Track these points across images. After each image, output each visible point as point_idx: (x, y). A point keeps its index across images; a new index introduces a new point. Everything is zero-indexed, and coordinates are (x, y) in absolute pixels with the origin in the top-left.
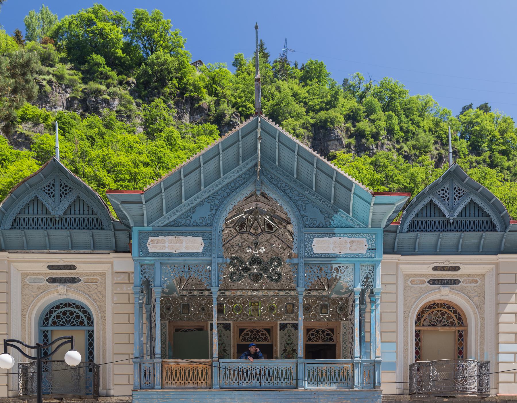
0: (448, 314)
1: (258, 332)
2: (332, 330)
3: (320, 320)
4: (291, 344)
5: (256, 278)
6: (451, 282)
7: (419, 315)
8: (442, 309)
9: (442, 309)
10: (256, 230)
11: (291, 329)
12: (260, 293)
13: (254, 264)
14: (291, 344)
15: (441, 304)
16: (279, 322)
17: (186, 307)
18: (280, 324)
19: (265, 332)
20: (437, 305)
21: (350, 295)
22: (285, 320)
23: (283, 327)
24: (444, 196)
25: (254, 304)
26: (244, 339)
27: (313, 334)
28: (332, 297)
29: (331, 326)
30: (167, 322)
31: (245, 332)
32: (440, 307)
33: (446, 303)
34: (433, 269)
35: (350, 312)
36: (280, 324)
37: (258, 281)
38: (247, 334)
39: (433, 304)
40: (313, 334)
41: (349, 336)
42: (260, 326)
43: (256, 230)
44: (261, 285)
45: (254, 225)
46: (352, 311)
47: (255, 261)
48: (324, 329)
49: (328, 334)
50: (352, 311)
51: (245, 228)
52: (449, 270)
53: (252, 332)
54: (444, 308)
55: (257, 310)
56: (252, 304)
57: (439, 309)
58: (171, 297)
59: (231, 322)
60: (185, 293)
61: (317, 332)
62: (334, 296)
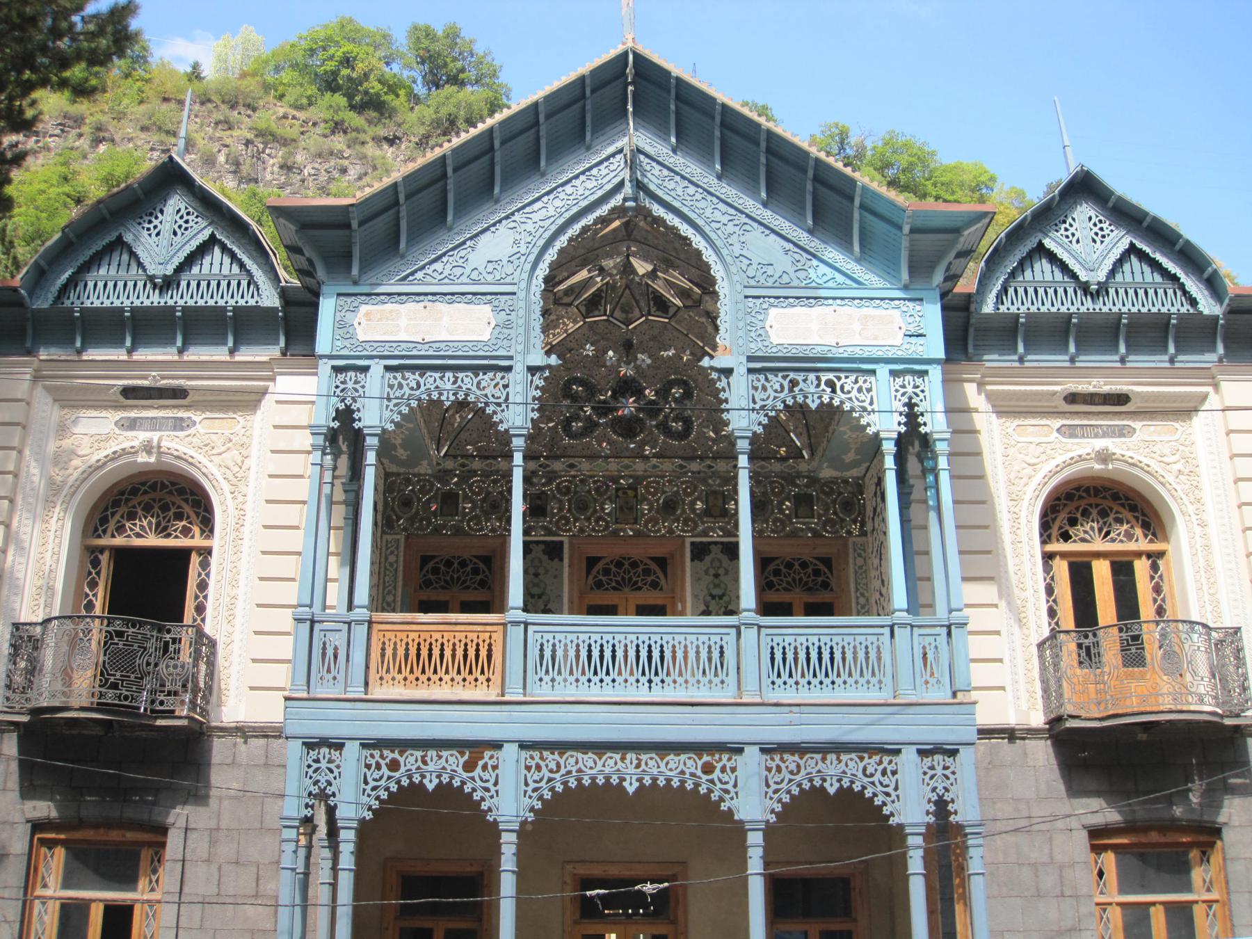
0: (1117, 512)
1: (634, 565)
2: (827, 562)
3: (794, 534)
4: (721, 597)
5: (628, 428)
6: (1113, 432)
7: (1044, 515)
8: (1099, 501)
9: (1099, 501)
10: (627, 312)
11: (720, 556)
12: (639, 467)
13: (623, 395)
14: (721, 597)
15: (1095, 488)
16: (688, 541)
17: (450, 501)
18: (692, 544)
19: (653, 566)
20: (1087, 490)
21: (868, 469)
22: (705, 533)
23: (700, 552)
24: (1069, 233)
25: (625, 493)
26: (599, 585)
27: (777, 573)
28: (821, 475)
29: (823, 551)
30: (402, 537)
31: (600, 565)
32: (1096, 496)
33: (1107, 484)
34: (1065, 399)
35: (869, 512)
36: (692, 544)
37: (636, 435)
38: (606, 572)
39: (1078, 489)
40: (777, 573)
41: (873, 573)
42: (638, 551)
43: (627, 312)
44: (641, 445)
45: (623, 300)
46: (875, 510)
47: (627, 387)
48: (805, 558)
49: (817, 572)
50: (875, 510)
51: (602, 308)
52: (1104, 404)
53: (619, 564)
54: (1104, 498)
55: (631, 509)
56: (620, 493)
57: (1092, 500)
58: (415, 475)
59: (566, 540)
60: (449, 464)
61: (789, 565)
62: (826, 473)
